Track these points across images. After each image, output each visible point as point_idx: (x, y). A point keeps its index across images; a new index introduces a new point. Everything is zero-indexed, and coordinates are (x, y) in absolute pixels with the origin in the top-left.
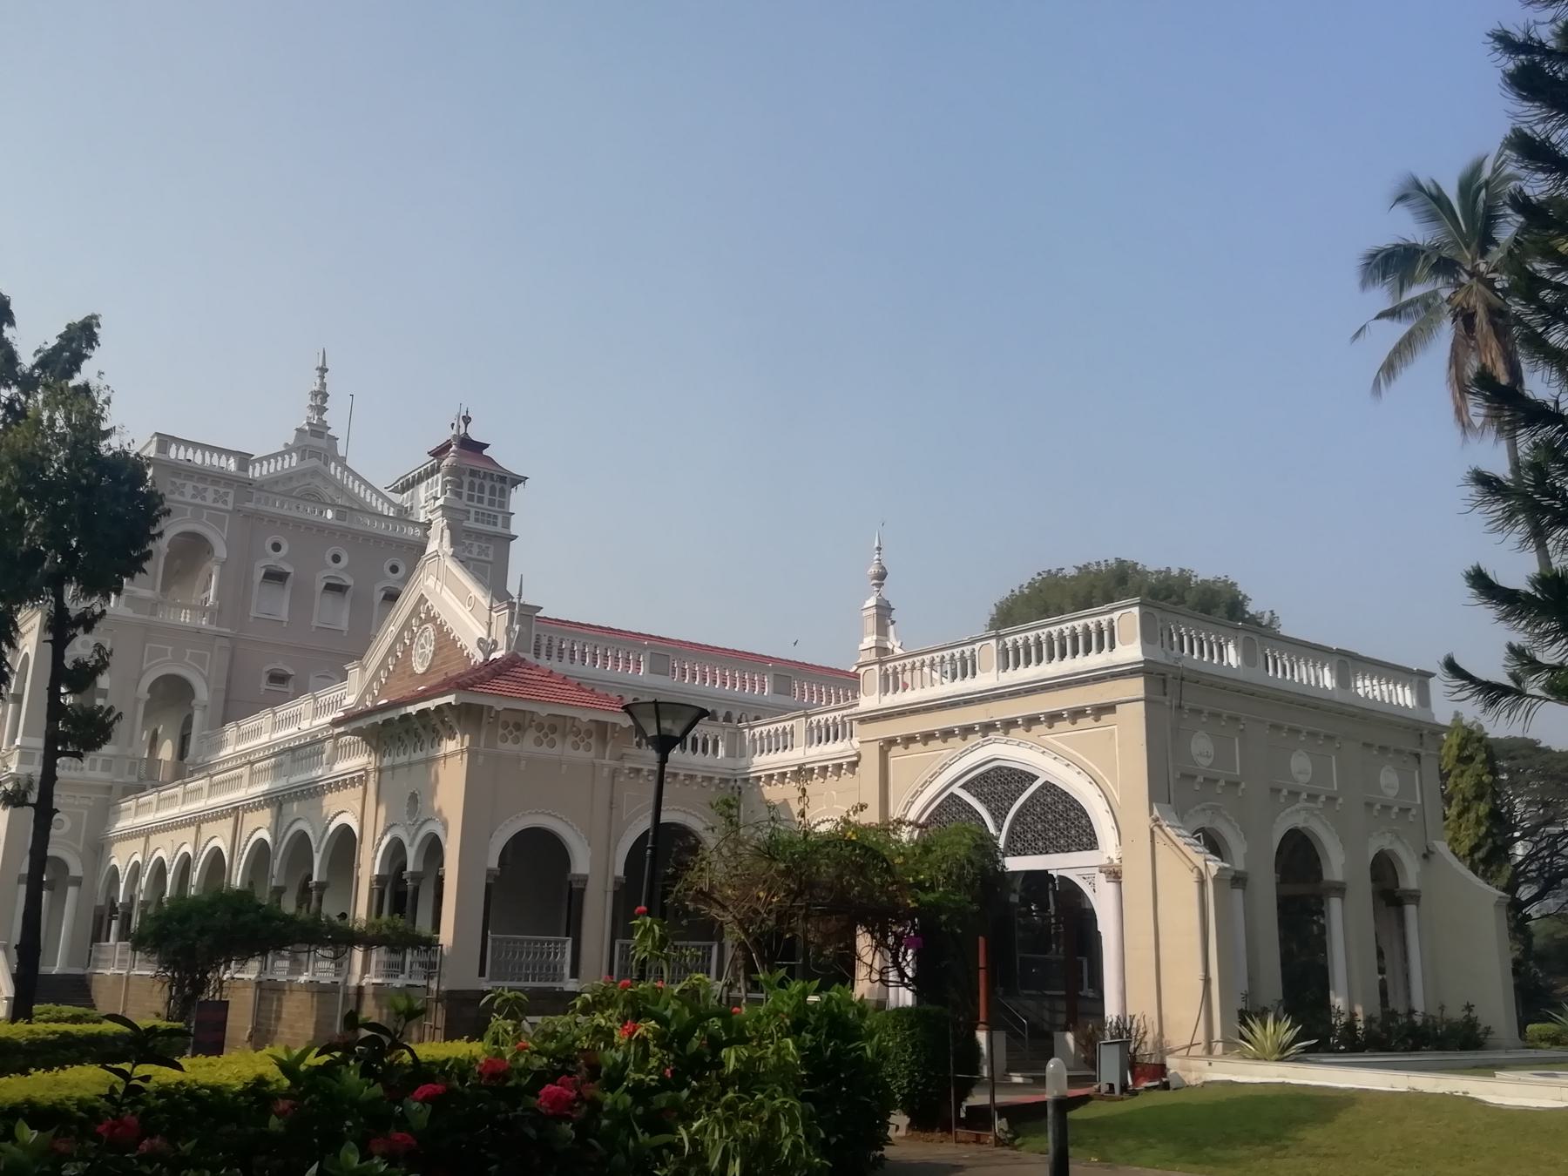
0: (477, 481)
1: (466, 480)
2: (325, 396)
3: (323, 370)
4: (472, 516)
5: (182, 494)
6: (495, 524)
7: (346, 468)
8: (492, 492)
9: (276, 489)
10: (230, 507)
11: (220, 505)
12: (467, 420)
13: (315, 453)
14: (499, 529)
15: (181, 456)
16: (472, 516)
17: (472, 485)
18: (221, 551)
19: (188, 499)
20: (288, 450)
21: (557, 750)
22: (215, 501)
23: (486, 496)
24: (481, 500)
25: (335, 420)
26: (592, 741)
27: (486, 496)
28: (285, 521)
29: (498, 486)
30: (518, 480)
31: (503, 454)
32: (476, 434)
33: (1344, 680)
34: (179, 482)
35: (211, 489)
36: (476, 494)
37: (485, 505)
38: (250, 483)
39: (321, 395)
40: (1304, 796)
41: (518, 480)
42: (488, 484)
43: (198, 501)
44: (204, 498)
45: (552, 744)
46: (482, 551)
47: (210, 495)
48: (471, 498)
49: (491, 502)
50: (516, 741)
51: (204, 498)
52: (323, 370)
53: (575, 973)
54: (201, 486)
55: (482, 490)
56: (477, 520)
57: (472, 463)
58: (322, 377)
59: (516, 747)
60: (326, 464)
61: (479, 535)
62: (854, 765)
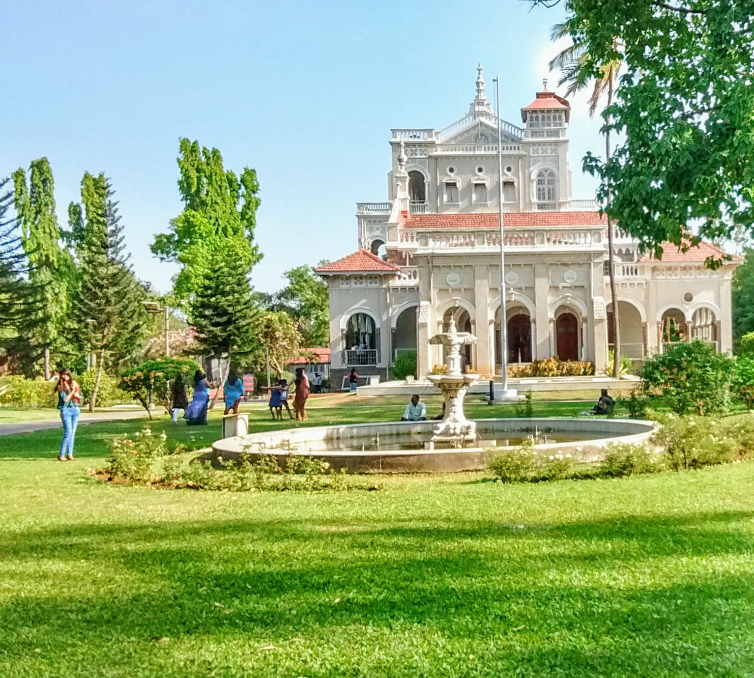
0: (546, 115)
1: (540, 115)
6: (558, 136)
14: (561, 138)
20: (467, 116)
21: (364, 285)
24: (549, 125)
28: (454, 157)
42: (552, 115)
45: (361, 283)
50: (347, 284)
53: (380, 361)
54: (414, 149)
55: (549, 118)
56: (548, 136)
61: (550, 143)
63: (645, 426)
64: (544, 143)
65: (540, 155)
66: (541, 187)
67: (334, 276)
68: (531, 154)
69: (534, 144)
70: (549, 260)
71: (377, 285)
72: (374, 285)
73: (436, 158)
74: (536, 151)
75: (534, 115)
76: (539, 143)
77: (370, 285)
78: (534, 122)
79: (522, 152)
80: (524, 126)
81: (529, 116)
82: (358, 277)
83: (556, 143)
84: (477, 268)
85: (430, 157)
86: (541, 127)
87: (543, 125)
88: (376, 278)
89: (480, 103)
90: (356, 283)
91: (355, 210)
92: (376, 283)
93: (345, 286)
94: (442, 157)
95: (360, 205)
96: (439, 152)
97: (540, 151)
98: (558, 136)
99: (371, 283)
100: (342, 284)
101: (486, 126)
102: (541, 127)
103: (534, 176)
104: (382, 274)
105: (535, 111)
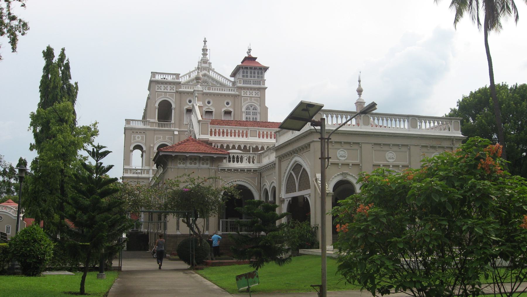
0: (253, 71)
1: (249, 71)
2: (207, 50)
3: (205, 42)
4: (252, 82)
5: (161, 89)
6: (260, 84)
7: (215, 72)
8: (258, 73)
9: (191, 84)
10: (175, 91)
11: (172, 91)
12: (250, 50)
13: (205, 69)
14: (262, 86)
15: (159, 78)
16: (252, 82)
17: (251, 73)
18: (173, 106)
19: (162, 90)
21: (197, 165)
22: (171, 90)
23: (256, 75)
24: (254, 77)
25: (210, 57)
26: (209, 162)
27: (256, 75)
29: (260, 71)
30: (266, 69)
31: (262, 61)
32: (253, 55)
33: (413, 125)
34: (159, 86)
35: (169, 86)
36: (253, 75)
37: (256, 78)
38: (180, 83)
39: (205, 50)
40: (391, 166)
41: (266, 69)
42: (256, 71)
43: (166, 91)
44: (167, 90)
45: (195, 164)
46: (256, 94)
47: (169, 88)
48: (251, 77)
49: (258, 77)
50: (183, 164)
51: (167, 90)
52: (205, 42)
54: (166, 86)
55: (254, 73)
56: (253, 84)
57: (252, 64)
58: (205, 44)
59: (184, 165)
60: (209, 72)
61: (255, 89)
62: (275, 164)
63: (224, 262)
64: (251, 89)
65: (248, 95)
66: (248, 116)
67: (176, 156)
68: (242, 95)
69: (244, 88)
70: (424, 143)
71: (208, 166)
72: (205, 166)
73: (181, 93)
74: (246, 93)
75: (245, 70)
76: (248, 88)
77: (202, 166)
78: (245, 74)
79: (237, 93)
80: (232, 79)
81: (241, 71)
82: (195, 159)
83: (259, 89)
84: (363, 145)
85: (177, 92)
86: (249, 78)
87: (251, 77)
88: (207, 160)
89: (204, 61)
90: (191, 164)
91: (123, 124)
92: (207, 164)
93: (181, 166)
94: (184, 92)
95: (128, 121)
96: (182, 89)
97: (248, 93)
98: (260, 84)
99: (203, 164)
100: (180, 163)
101: (209, 77)
102: (249, 78)
103: (244, 109)
104: (215, 156)
105: (247, 68)
